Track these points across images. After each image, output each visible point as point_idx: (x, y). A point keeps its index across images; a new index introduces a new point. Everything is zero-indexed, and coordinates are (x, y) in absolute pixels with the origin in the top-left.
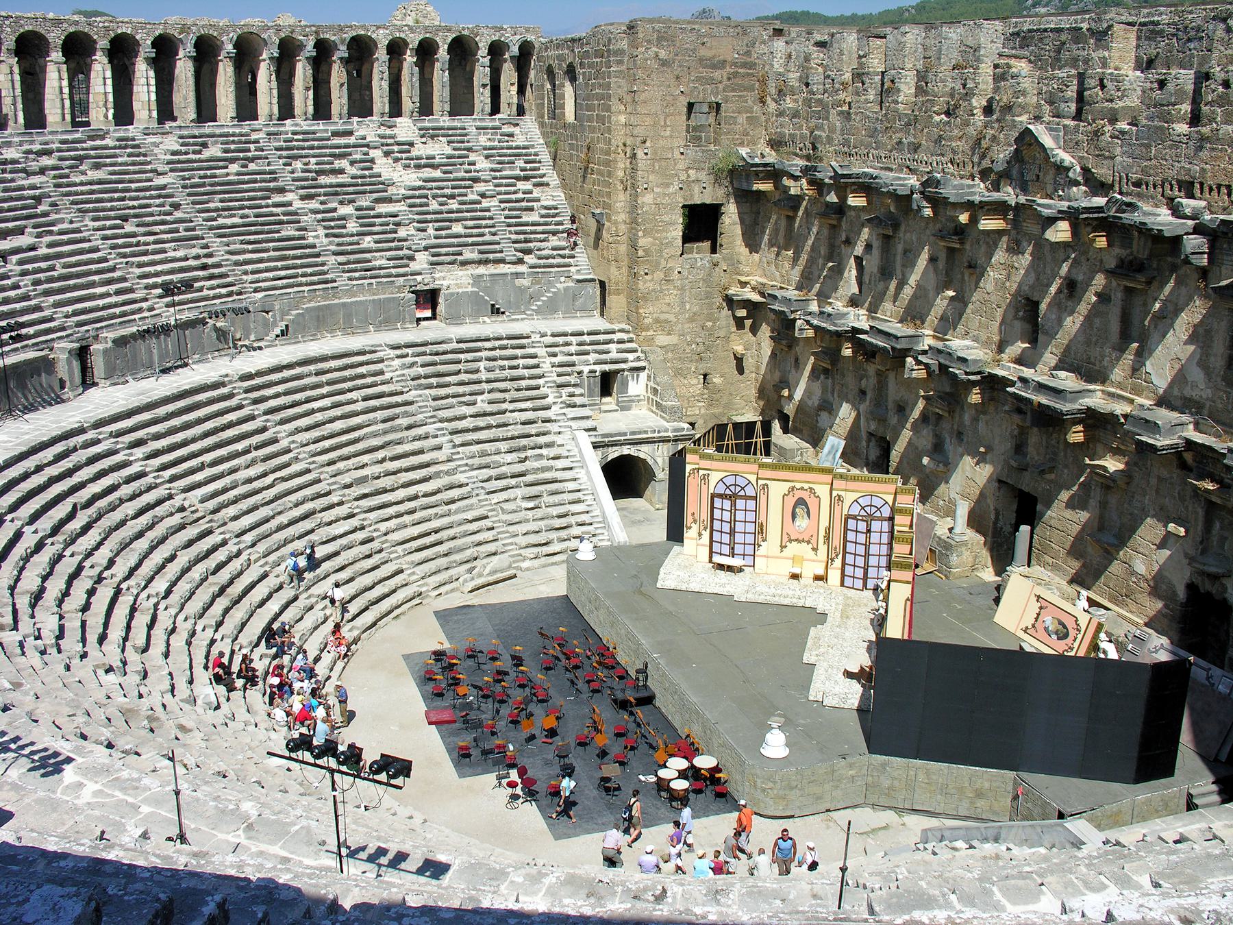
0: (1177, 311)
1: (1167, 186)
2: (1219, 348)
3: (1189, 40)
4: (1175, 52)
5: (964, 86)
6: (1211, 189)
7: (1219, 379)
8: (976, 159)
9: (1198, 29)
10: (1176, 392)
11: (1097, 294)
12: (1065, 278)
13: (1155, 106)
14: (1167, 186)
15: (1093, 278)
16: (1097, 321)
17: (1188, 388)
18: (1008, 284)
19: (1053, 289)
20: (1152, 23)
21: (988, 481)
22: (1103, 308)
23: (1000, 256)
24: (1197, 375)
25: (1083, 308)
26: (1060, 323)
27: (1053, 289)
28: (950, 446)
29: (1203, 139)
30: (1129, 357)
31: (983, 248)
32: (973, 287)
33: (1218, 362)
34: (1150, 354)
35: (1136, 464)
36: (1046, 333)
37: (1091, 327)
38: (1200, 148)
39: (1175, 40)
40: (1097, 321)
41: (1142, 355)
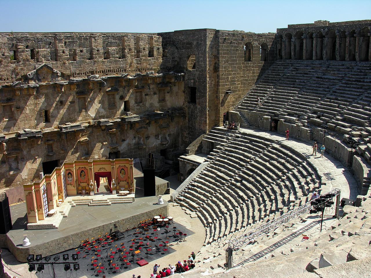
0: (94, 99)
1: (87, 73)
2: (106, 103)
3: (39, 41)
4: (34, 44)
5: (3, 55)
6: (98, 72)
7: (107, 109)
8: (14, 76)
9: (42, 39)
10: (97, 116)
11: (70, 102)
12: (59, 101)
13: (81, 56)
14: (87, 73)
15: (68, 99)
16: (71, 109)
17: (101, 114)
18: (36, 109)
19: (54, 105)
20: (26, 37)
21: (39, 165)
22: (72, 105)
23: (31, 101)
24: (102, 110)
25: (66, 107)
26: (58, 113)
27: (54, 105)
28: (14, 165)
29: (95, 62)
30: (84, 113)
31: (22, 102)
32: (20, 114)
33: (107, 106)
34: (89, 110)
35: (90, 136)
36: (52, 117)
37: (70, 110)
38: (95, 64)
39: (34, 41)
40: (71, 109)
41: (86, 111)
